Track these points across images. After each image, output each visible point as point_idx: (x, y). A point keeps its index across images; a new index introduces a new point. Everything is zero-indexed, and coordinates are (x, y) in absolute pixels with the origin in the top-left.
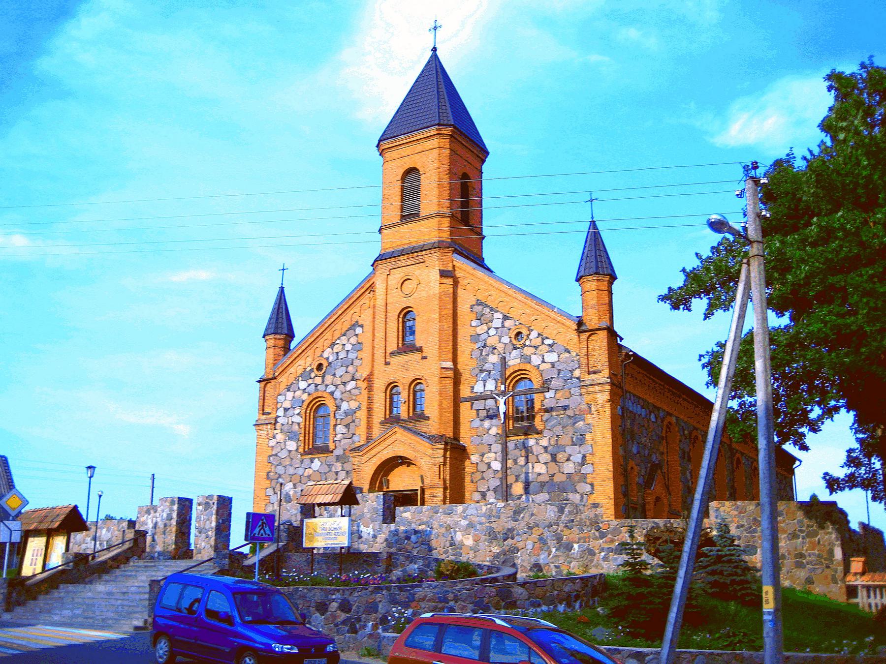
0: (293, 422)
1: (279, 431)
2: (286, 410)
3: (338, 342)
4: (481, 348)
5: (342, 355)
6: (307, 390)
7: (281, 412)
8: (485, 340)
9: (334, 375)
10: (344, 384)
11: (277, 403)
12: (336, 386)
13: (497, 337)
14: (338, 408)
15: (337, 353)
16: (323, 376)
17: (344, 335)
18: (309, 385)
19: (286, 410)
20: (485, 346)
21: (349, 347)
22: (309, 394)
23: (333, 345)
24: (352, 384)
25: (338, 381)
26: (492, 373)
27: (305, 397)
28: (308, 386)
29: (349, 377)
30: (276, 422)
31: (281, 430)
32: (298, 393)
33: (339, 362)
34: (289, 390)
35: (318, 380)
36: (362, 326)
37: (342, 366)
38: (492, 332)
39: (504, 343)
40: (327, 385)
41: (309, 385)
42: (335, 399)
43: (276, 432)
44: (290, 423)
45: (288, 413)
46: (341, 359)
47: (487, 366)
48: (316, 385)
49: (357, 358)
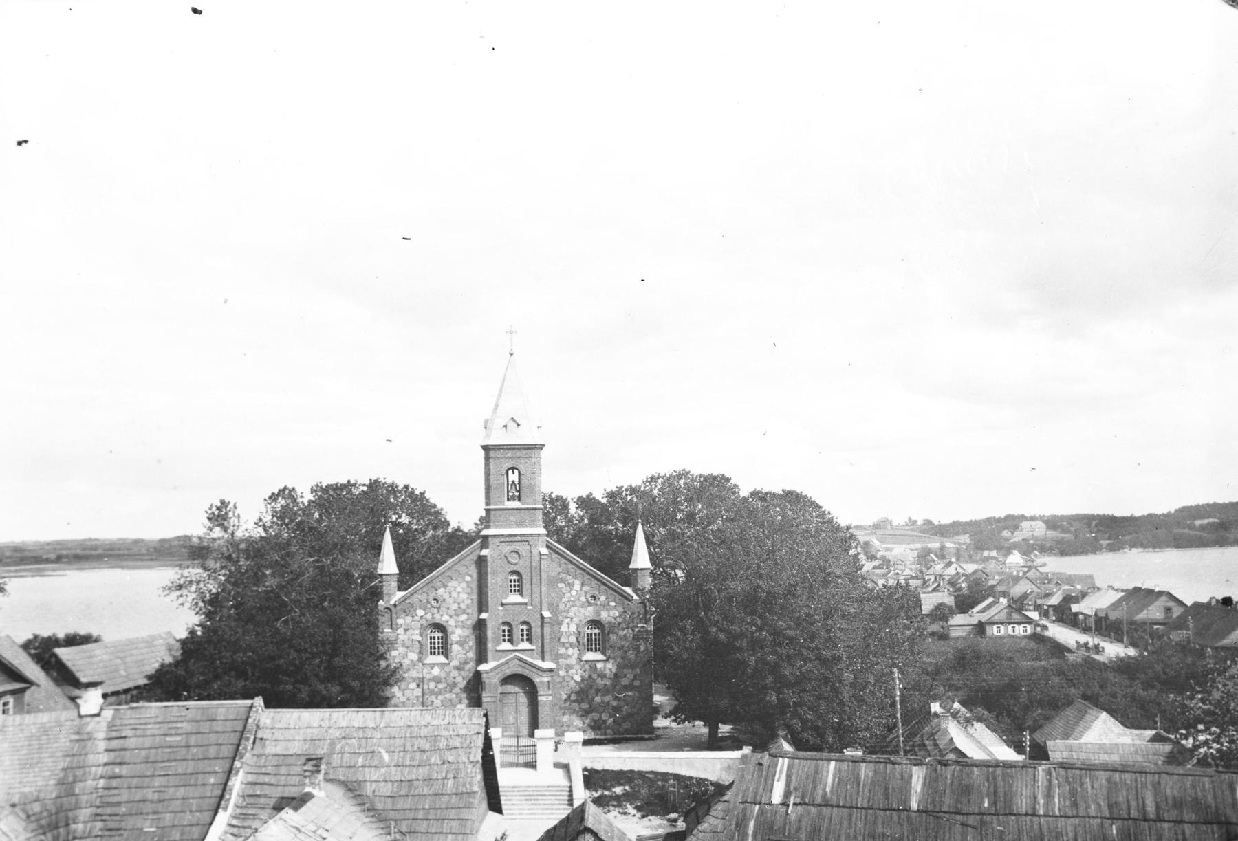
5: (454, 595)
9: (448, 608)
10: (458, 615)
12: (451, 617)
15: (450, 593)
16: (438, 608)
19: (406, 630)
21: (459, 589)
27: (423, 622)
36: (471, 576)
37: (455, 602)
40: (442, 615)
47: (571, 614)
48: (433, 615)
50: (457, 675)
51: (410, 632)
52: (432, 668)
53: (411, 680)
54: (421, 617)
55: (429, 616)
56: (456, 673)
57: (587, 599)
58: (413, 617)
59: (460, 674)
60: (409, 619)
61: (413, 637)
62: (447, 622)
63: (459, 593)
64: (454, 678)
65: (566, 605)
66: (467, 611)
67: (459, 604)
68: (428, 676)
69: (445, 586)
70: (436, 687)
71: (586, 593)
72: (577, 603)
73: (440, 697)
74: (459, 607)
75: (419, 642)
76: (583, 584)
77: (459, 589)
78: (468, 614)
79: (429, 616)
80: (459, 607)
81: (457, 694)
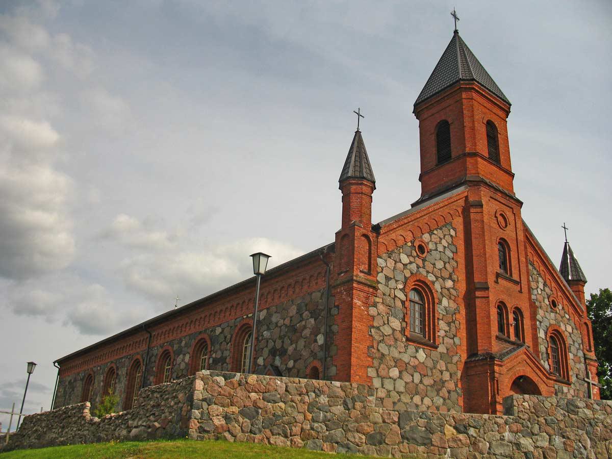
1: (381, 300)
3: (435, 232)
5: (440, 248)
10: (444, 279)
12: (437, 277)
16: (424, 260)
17: (441, 229)
18: (411, 263)
19: (388, 279)
22: (412, 273)
23: (431, 233)
24: (449, 284)
26: (542, 324)
28: (409, 263)
29: (446, 275)
32: (400, 266)
33: (438, 256)
34: (390, 257)
35: (420, 262)
36: (454, 229)
37: (440, 259)
40: (428, 272)
41: (411, 263)
46: (440, 252)
48: (418, 267)
49: (453, 259)
50: (444, 368)
51: (392, 283)
53: (393, 364)
54: (405, 265)
55: (413, 267)
56: (442, 365)
57: (550, 304)
59: (447, 370)
60: (391, 263)
62: (433, 283)
63: (445, 247)
64: (441, 372)
67: (445, 263)
68: (413, 362)
69: (431, 233)
70: (421, 382)
74: (445, 267)
75: (403, 302)
76: (545, 285)
77: (444, 243)
78: (453, 281)
79: (413, 267)
80: (445, 267)
81: (444, 399)
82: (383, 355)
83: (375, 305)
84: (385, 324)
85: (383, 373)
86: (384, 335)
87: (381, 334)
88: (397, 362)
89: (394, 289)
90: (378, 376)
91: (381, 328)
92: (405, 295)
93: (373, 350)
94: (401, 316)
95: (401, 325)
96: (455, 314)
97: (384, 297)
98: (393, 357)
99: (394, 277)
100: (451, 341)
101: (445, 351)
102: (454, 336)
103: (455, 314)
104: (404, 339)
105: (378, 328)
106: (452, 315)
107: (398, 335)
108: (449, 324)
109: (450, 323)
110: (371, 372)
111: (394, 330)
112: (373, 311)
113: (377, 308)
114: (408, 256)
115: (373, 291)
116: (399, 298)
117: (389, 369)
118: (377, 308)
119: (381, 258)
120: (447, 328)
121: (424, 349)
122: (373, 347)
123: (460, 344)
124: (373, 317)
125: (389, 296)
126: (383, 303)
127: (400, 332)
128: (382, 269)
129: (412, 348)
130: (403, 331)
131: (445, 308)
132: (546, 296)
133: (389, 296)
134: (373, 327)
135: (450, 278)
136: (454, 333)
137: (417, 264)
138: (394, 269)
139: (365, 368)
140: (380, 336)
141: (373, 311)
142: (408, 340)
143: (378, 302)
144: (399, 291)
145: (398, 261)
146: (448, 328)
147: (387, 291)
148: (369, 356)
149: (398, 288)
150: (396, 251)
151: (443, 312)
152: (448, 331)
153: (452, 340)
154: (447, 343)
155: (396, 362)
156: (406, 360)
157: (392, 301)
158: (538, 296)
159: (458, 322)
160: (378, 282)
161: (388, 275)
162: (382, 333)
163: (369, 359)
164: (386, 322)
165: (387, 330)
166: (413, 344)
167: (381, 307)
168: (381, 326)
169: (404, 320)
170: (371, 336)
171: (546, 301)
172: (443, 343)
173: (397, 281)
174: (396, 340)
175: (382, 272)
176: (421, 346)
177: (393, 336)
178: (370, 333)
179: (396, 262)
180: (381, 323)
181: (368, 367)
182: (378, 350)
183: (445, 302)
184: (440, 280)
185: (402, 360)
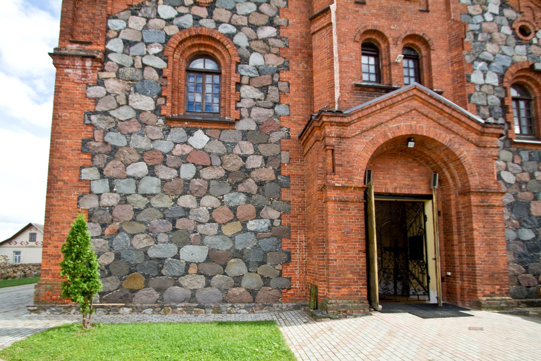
0: (144, 66)
1: (114, 75)
2: (127, 44)
4: (477, 32)
6: (175, 22)
7: (116, 45)
8: (480, 24)
11: (108, 29)
13: (495, 26)
14: (245, 60)
18: (180, 15)
19: (127, 44)
20: (481, 30)
22: (181, 28)
24: (269, 32)
25: (243, 21)
27: (172, 30)
28: (177, 16)
30: (106, 59)
31: (117, 74)
32: (155, 22)
34: (134, 14)
38: (488, 17)
39: (506, 35)
42: (239, 47)
43: (104, 75)
44: (139, 64)
45: (132, 49)
48: (197, 19)
52: (190, 133)
55: (188, 21)
57: (514, 33)
58: (148, 19)
60: (137, 22)
61: (146, 61)
62: (231, 36)
65: (476, 36)
66: (280, 21)
71: (511, 22)
72: (496, 35)
73: (209, 201)
75: (160, 71)
79: (188, 21)
82: (115, 149)
83: (100, 83)
84: (119, 106)
85: (111, 170)
86: (117, 121)
87: (113, 120)
88: (142, 155)
89: (142, 56)
90: (103, 176)
91: (112, 113)
92: (164, 60)
93: (93, 144)
94: (157, 90)
95: (156, 102)
96: (278, 72)
97: (121, 69)
98: (136, 149)
99: (142, 40)
100: (271, 112)
101: (253, 127)
102: (275, 104)
103: (278, 72)
104: (161, 121)
105: (106, 113)
106: (273, 76)
107: (152, 118)
108: (264, 89)
109: (267, 87)
110: (89, 174)
111: (139, 112)
112: (95, 91)
113: (105, 87)
114: (174, 7)
115: (92, 64)
116: (153, 67)
117: (127, 165)
118: (105, 87)
119: (116, 18)
120: (259, 95)
121: (204, 130)
122: (93, 139)
123: (288, 113)
124: (96, 100)
125: (133, 66)
126: (118, 77)
127: (154, 112)
128: (119, 32)
129: (178, 133)
130: (157, 110)
131: (257, 68)
132: (505, 22)
133: (133, 66)
134: (95, 113)
135: (271, 23)
136: (276, 99)
137: (194, 16)
138: (143, 29)
139: (76, 169)
140: (111, 123)
141: (95, 91)
142: (168, 120)
143: (106, 79)
144: (154, 57)
145: (152, 16)
146: (262, 94)
147: (127, 60)
148: (85, 153)
149: (151, 53)
150: (147, 3)
151: (251, 72)
152: (263, 98)
153: (271, 110)
154: (259, 115)
155: (142, 155)
156: (165, 149)
157: (139, 72)
158: (485, 25)
159: (285, 84)
160: (107, 52)
161: (129, 39)
162: (114, 118)
163: (85, 156)
164: (124, 102)
165: (124, 113)
166: (179, 125)
167: (112, 84)
168: (111, 110)
169: (160, 95)
170: (92, 125)
171: (506, 30)
172: (249, 117)
173: (147, 44)
174: (144, 125)
175: (117, 36)
176: (199, 126)
177: (137, 118)
178: (88, 122)
179: (148, 19)
180: (113, 104)
181: (82, 167)
182: (106, 143)
183: (256, 59)
184: (249, 30)
185: (156, 151)
